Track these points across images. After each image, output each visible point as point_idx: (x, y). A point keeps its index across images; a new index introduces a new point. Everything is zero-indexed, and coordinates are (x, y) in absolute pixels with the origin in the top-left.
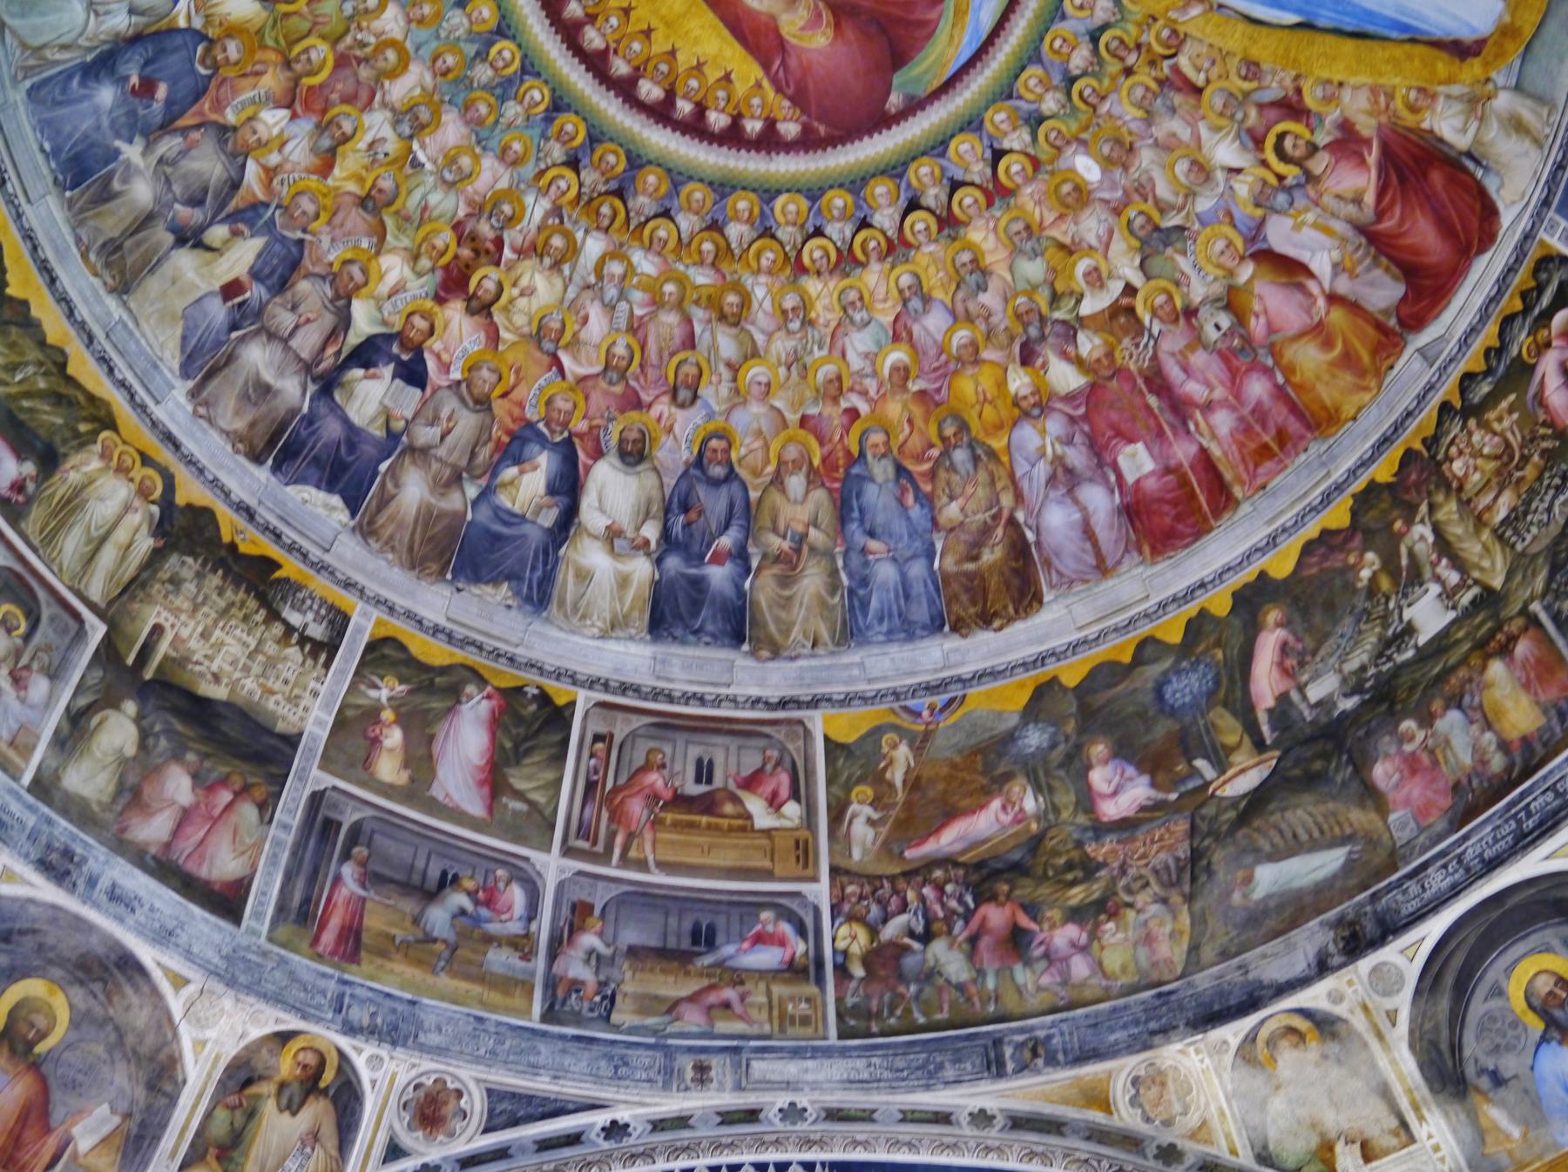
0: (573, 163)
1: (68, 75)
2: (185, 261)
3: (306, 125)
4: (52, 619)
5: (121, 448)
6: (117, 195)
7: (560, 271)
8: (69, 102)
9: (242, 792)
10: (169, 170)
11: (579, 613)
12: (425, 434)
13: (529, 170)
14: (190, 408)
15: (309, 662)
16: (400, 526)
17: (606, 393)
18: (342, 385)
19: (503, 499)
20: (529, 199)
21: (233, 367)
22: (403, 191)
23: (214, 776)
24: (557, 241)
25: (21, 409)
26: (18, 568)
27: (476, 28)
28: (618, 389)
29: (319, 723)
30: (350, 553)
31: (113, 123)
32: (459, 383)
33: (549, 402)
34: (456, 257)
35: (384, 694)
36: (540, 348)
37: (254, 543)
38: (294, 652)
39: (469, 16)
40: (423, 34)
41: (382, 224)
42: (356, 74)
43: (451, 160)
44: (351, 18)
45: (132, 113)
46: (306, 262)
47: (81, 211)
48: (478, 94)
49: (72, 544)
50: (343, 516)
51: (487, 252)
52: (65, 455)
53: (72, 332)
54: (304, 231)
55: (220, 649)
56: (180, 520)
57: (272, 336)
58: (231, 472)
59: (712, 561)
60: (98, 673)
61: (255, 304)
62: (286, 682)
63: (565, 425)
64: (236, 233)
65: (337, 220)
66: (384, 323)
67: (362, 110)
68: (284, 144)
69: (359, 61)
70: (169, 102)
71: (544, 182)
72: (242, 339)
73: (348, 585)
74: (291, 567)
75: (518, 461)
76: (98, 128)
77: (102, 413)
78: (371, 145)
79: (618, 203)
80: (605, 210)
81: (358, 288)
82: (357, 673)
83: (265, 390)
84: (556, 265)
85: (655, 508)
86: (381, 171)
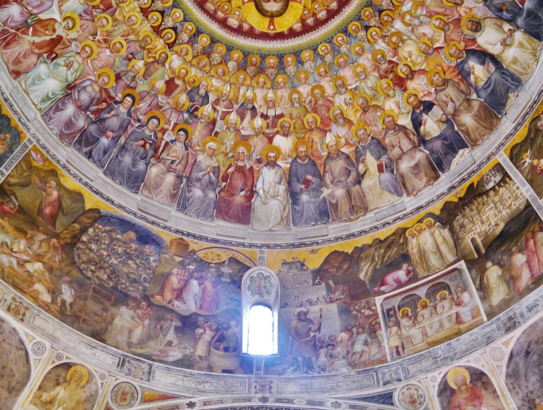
0: (367, 28)
1: (294, 210)
2: (366, 183)
3: (334, 127)
4: (450, 280)
5: (413, 229)
6: (337, 202)
7: (405, 40)
8: (303, 211)
9: (534, 233)
10: (336, 180)
11: (527, 68)
12: (450, 108)
13: (367, 46)
14: (412, 197)
15: (507, 185)
16: (477, 129)
17: (452, 32)
18: (424, 136)
19: (481, 84)
20: (377, 47)
21: (405, 176)
22: (364, 95)
23: (523, 243)
24: (394, 39)
25: (387, 261)
26: (430, 285)
27: (312, 59)
28: (452, 27)
29: (528, 191)
30: (478, 154)
31: (314, 197)
32: (436, 90)
33: (451, 56)
34: (391, 80)
35: (528, 160)
36: (431, 54)
37: (462, 191)
38: (502, 190)
39: (307, 61)
40: (311, 79)
41: (373, 106)
42: (320, 106)
43: (358, 75)
44: (300, 105)
45: (313, 189)
46: (380, 138)
47: (337, 217)
48: (336, 61)
49: (434, 261)
50: (467, 150)
51: (392, 67)
52: (407, 251)
53: (371, 234)
54: (369, 136)
55: (489, 218)
56: (444, 216)
57: (400, 158)
58: (437, 189)
59: (523, 5)
60: (474, 271)
61: (388, 161)
62: (510, 198)
63: (461, 51)
64: (363, 162)
65: (368, 122)
66: (408, 113)
67: (333, 105)
68: (339, 136)
69: (316, 103)
70: (314, 175)
71: (372, 41)
72: (397, 170)
73: (489, 158)
74: (475, 179)
75: (469, 74)
76: (314, 203)
77: (400, 232)
78: (346, 104)
79: (384, 13)
80: (386, 18)
81: (393, 120)
82: (517, 168)
83: (417, 166)
84: (403, 41)
85: (498, 23)
86: (355, 102)
